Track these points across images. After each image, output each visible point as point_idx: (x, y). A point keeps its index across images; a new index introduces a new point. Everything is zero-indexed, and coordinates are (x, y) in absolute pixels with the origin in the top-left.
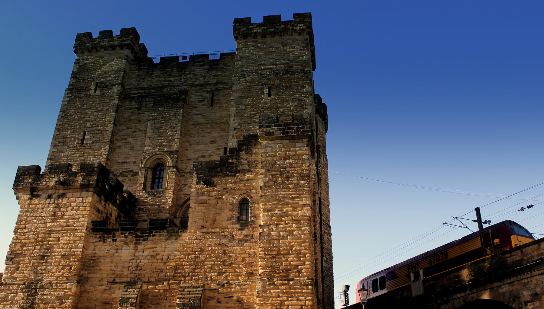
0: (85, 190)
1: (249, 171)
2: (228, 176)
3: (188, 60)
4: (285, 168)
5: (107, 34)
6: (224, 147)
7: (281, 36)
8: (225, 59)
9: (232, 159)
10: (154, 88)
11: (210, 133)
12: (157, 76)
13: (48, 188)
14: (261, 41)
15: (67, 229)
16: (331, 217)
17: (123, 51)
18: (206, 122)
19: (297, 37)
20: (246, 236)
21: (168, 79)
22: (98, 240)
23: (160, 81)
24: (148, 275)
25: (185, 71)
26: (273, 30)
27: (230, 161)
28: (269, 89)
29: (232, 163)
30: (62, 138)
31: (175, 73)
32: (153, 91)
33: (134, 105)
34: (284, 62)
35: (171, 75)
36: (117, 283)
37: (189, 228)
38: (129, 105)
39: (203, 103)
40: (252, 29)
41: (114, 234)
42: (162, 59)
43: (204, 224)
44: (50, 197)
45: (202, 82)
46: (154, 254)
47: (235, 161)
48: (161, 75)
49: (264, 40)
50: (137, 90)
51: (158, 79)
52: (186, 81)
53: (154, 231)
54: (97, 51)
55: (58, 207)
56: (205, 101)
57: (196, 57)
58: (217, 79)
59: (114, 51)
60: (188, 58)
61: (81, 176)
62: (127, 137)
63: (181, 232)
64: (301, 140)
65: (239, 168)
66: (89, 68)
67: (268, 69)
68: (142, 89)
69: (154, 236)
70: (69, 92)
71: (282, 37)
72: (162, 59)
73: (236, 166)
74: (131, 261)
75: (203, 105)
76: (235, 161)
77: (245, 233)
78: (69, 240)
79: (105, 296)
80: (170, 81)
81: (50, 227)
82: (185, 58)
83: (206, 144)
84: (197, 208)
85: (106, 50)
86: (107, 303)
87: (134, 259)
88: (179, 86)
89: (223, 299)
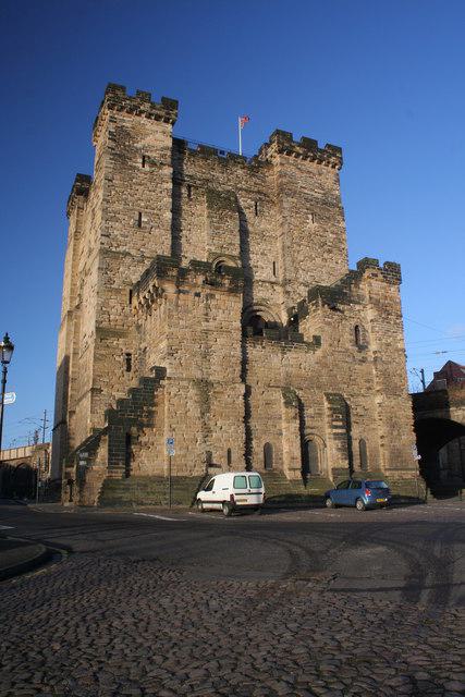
1: (359, 303)
12: (201, 167)
15: (221, 329)
44: (198, 295)
55: (208, 307)
66: (129, 134)
72: (200, 146)
77: (362, 355)
82: (222, 152)
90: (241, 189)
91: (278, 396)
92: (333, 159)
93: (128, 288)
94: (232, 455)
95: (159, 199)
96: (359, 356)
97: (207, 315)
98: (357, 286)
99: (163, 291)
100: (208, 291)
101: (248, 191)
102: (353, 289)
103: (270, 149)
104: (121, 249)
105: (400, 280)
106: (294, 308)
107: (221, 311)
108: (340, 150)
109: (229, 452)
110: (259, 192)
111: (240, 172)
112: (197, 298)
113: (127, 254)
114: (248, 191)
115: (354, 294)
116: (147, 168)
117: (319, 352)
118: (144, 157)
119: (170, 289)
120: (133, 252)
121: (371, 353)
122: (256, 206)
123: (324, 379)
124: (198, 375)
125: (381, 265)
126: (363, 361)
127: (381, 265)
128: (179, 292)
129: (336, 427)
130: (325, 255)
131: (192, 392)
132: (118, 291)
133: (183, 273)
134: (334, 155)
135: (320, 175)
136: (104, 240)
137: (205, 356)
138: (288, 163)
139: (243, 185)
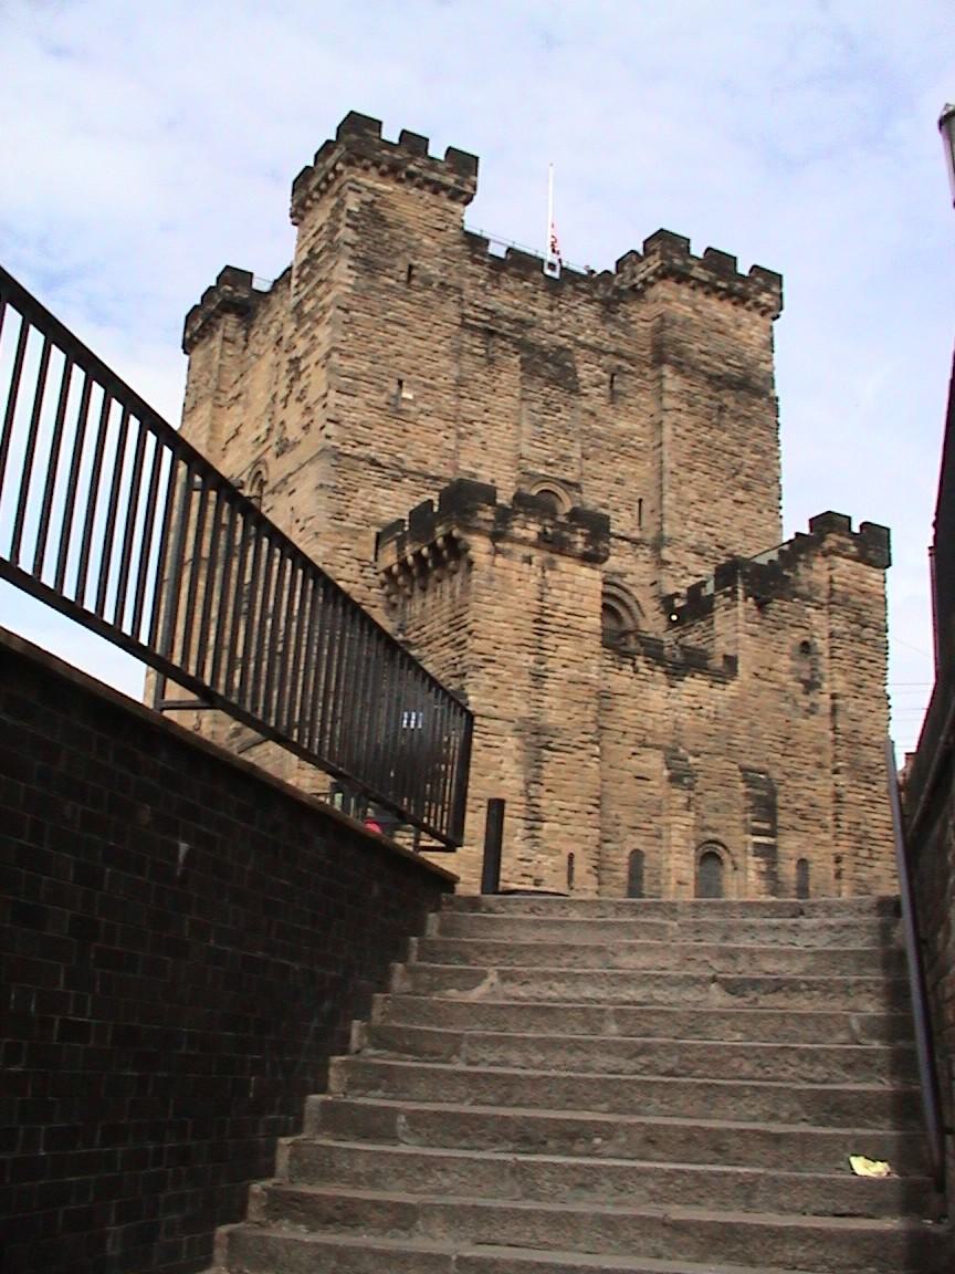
0: (588, 564)
3: (556, 275)
4: (860, 610)
5: (413, 143)
7: (735, 304)
8: (623, 302)
10: (507, 319)
12: (511, 293)
13: (523, 541)
15: (568, 632)
19: (758, 317)
20: (813, 704)
27: (785, 573)
30: (353, 378)
35: (535, 300)
37: (739, 673)
40: (691, 267)
44: (528, 560)
45: (590, 341)
47: (791, 574)
49: (708, 301)
52: (563, 325)
55: (543, 584)
57: (578, 277)
61: (582, 535)
62: (474, 418)
65: (799, 589)
68: (486, 311)
70: (351, 263)
71: (736, 308)
72: (510, 250)
75: (600, 395)
77: (812, 698)
78: (577, 655)
80: (534, 314)
83: (608, 481)
84: (748, 642)
90: (584, 346)
91: (654, 762)
92: (764, 298)
93: (375, 530)
94: (576, 866)
99: (467, 549)
101: (598, 350)
103: (642, 266)
104: (359, 450)
106: (677, 595)
107: (566, 593)
108: (777, 279)
109: (571, 857)
110: (618, 354)
112: (526, 565)
113: (373, 462)
115: (804, 580)
117: (733, 686)
120: (384, 459)
121: (826, 697)
122: (612, 381)
123: (741, 740)
124: (524, 710)
125: (855, 528)
126: (812, 710)
127: (855, 528)
128: (497, 552)
129: (757, 832)
130: (740, 495)
131: (512, 742)
132: (354, 534)
133: (504, 516)
134: (767, 290)
135: (739, 327)
136: (331, 429)
137: (538, 678)
138: (679, 300)
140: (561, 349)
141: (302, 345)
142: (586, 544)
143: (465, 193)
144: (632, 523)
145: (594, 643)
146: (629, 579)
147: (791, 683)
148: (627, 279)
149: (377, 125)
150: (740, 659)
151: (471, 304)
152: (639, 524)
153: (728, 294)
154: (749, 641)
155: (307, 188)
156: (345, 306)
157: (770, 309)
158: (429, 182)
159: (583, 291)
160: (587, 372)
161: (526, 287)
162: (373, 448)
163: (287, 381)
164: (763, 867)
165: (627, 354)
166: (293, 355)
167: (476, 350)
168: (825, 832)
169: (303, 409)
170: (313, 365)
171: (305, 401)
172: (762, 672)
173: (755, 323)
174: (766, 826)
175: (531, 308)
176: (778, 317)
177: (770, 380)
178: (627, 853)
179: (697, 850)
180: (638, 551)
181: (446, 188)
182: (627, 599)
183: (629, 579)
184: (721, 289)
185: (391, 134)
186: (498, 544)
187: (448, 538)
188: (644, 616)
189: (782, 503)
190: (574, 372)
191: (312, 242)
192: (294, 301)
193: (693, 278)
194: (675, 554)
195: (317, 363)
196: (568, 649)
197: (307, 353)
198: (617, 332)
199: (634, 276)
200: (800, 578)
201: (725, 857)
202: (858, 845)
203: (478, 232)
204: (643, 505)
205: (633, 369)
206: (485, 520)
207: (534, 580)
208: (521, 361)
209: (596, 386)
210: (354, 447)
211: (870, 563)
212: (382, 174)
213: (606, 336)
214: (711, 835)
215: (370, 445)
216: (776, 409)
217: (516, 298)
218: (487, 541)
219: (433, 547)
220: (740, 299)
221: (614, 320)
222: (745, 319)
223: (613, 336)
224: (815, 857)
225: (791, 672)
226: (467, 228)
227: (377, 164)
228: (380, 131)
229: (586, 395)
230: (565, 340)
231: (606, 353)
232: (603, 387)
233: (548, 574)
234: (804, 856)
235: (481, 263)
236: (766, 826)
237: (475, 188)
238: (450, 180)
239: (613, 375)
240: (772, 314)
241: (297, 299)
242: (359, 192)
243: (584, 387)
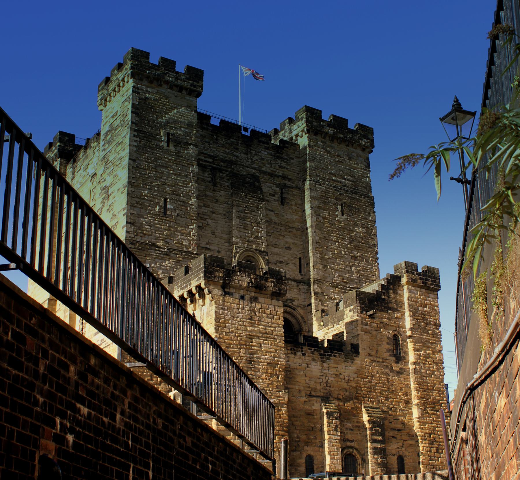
1: (397, 310)
2: (382, 311)
3: (248, 134)
6: (299, 257)
9: (384, 296)
10: (222, 161)
11: (284, 236)
12: (223, 146)
13: (240, 287)
14: (329, 143)
15: (266, 335)
16: (19, 287)
17: (191, 99)
18: (279, 222)
19: (360, 152)
20: (401, 369)
21: (235, 154)
22: (290, 352)
23: (227, 154)
24: (337, 392)
25: (251, 149)
26: (342, 136)
27: (383, 297)
28: (342, 205)
29: (384, 299)
30: (139, 198)
31: (242, 149)
32: (222, 164)
33: (206, 177)
34: (351, 178)
35: (237, 149)
36: (314, 396)
37: (360, 354)
38: (202, 176)
39: (275, 198)
41: (302, 348)
42: (222, 122)
43: (370, 352)
44: (242, 297)
45: (269, 171)
46: (338, 373)
47: (386, 297)
48: (227, 146)
49: (332, 145)
50: (205, 157)
51: (224, 149)
52: (253, 162)
53: (334, 352)
54: (161, 85)
55: (252, 310)
56: (276, 196)
58: (283, 171)
59: (180, 94)
60: (249, 130)
61: (272, 282)
63: (355, 356)
64: (432, 292)
65: (390, 305)
66: (152, 107)
67: (338, 181)
68: (210, 156)
69: (335, 356)
70: (136, 134)
72: (222, 122)
73: (387, 303)
74: (321, 377)
75: (275, 200)
76: (386, 297)
77: (400, 366)
78: (271, 348)
79: (307, 407)
80: (237, 157)
81: (250, 331)
82: (246, 129)
83: (282, 248)
85: (171, 88)
86: (309, 414)
87: (323, 375)
88: (248, 167)
89: (393, 420)
90: (265, 173)
92: (364, 142)
95: (185, 184)
96: (396, 367)
97: (251, 319)
98: (395, 293)
100: (253, 294)
101: (272, 175)
102: (392, 295)
103: (295, 127)
105: (439, 286)
111: (264, 153)
114: (272, 175)
115: (393, 301)
116: (172, 148)
118: (168, 134)
119: (218, 292)
125: (420, 270)
133: (229, 273)
139: (267, 168)
140: (253, 176)
141: (109, 180)
142: (275, 286)
143: (196, 91)
144: (297, 272)
145: (281, 342)
146: (295, 303)
147: (389, 358)
148: (287, 134)
149: (147, 55)
150: (360, 346)
151: (202, 153)
152: (300, 272)
153: (342, 141)
154: (365, 337)
155: (108, 90)
156: (134, 158)
157: (367, 147)
158: (177, 86)
159: (263, 142)
160: (267, 187)
161: (232, 142)
162: (153, 237)
163: (100, 200)
164: (379, 461)
165: (289, 177)
166: (103, 185)
167: (206, 178)
168: (412, 439)
169: (111, 216)
170: (116, 191)
171: (112, 212)
172: (373, 353)
173: (359, 156)
174: (380, 438)
175: (235, 154)
176: (372, 151)
177: (369, 188)
178: (304, 455)
179: (342, 451)
180: (300, 286)
181: (186, 89)
182: (295, 313)
183: (295, 303)
184: (340, 138)
185: (154, 60)
186: (226, 290)
187: (199, 287)
188: (305, 322)
189: (378, 256)
190: (261, 190)
191: (112, 120)
192: (102, 154)
193: (323, 132)
194: (321, 288)
195: (119, 190)
196: (266, 347)
197: (112, 184)
198: (284, 164)
199: (291, 132)
200: (391, 299)
201: (358, 456)
202: (431, 446)
203: (204, 112)
204: (302, 261)
205: (294, 185)
206: (219, 277)
207: (247, 308)
208: (231, 183)
209: (273, 195)
210: (141, 237)
211: (428, 289)
212: (151, 82)
213: (277, 167)
214: (349, 444)
215: (151, 235)
216: (373, 205)
217: (226, 148)
218: (220, 287)
219: (190, 292)
220: (349, 143)
221: (281, 158)
222: (353, 154)
223: (281, 167)
224: (407, 453)
225: (388, 350)
226: (198, 110)
227: (148, 77)
228: (148, 58)
229: (268, 201)
230: (254, 171)
231: (278, 177)
232: (276, 196)
233: (254, 304)
234: (401, 453)
235: (207, 129)
236: (380, 438)
237: (202, 87)
238: (187, 84)
239: (282, 190)
240: (368, 150)
241: (104, 153)
242: (139, 93)
243: (266, 196)
